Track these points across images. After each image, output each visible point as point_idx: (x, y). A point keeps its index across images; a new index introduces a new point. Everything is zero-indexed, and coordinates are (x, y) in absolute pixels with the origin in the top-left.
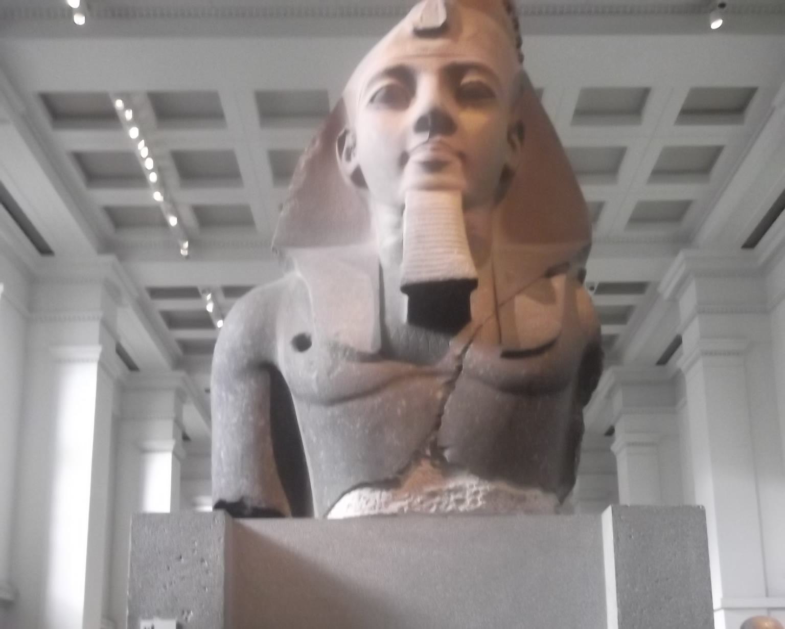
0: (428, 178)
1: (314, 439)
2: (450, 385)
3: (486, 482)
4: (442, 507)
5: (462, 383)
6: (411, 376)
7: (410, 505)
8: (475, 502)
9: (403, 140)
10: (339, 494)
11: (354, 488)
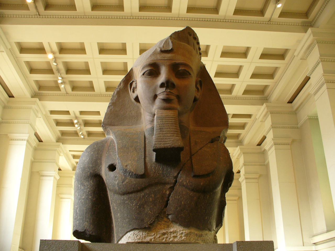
0: (165, 105)
1: (116, 208)
2: (172, 189)
3: (186, 229)
4: (167, 239)
5: (177, 187)
6: (156, 184)
8: (181, 237)
9: (155, 90)
11: (132, 230)
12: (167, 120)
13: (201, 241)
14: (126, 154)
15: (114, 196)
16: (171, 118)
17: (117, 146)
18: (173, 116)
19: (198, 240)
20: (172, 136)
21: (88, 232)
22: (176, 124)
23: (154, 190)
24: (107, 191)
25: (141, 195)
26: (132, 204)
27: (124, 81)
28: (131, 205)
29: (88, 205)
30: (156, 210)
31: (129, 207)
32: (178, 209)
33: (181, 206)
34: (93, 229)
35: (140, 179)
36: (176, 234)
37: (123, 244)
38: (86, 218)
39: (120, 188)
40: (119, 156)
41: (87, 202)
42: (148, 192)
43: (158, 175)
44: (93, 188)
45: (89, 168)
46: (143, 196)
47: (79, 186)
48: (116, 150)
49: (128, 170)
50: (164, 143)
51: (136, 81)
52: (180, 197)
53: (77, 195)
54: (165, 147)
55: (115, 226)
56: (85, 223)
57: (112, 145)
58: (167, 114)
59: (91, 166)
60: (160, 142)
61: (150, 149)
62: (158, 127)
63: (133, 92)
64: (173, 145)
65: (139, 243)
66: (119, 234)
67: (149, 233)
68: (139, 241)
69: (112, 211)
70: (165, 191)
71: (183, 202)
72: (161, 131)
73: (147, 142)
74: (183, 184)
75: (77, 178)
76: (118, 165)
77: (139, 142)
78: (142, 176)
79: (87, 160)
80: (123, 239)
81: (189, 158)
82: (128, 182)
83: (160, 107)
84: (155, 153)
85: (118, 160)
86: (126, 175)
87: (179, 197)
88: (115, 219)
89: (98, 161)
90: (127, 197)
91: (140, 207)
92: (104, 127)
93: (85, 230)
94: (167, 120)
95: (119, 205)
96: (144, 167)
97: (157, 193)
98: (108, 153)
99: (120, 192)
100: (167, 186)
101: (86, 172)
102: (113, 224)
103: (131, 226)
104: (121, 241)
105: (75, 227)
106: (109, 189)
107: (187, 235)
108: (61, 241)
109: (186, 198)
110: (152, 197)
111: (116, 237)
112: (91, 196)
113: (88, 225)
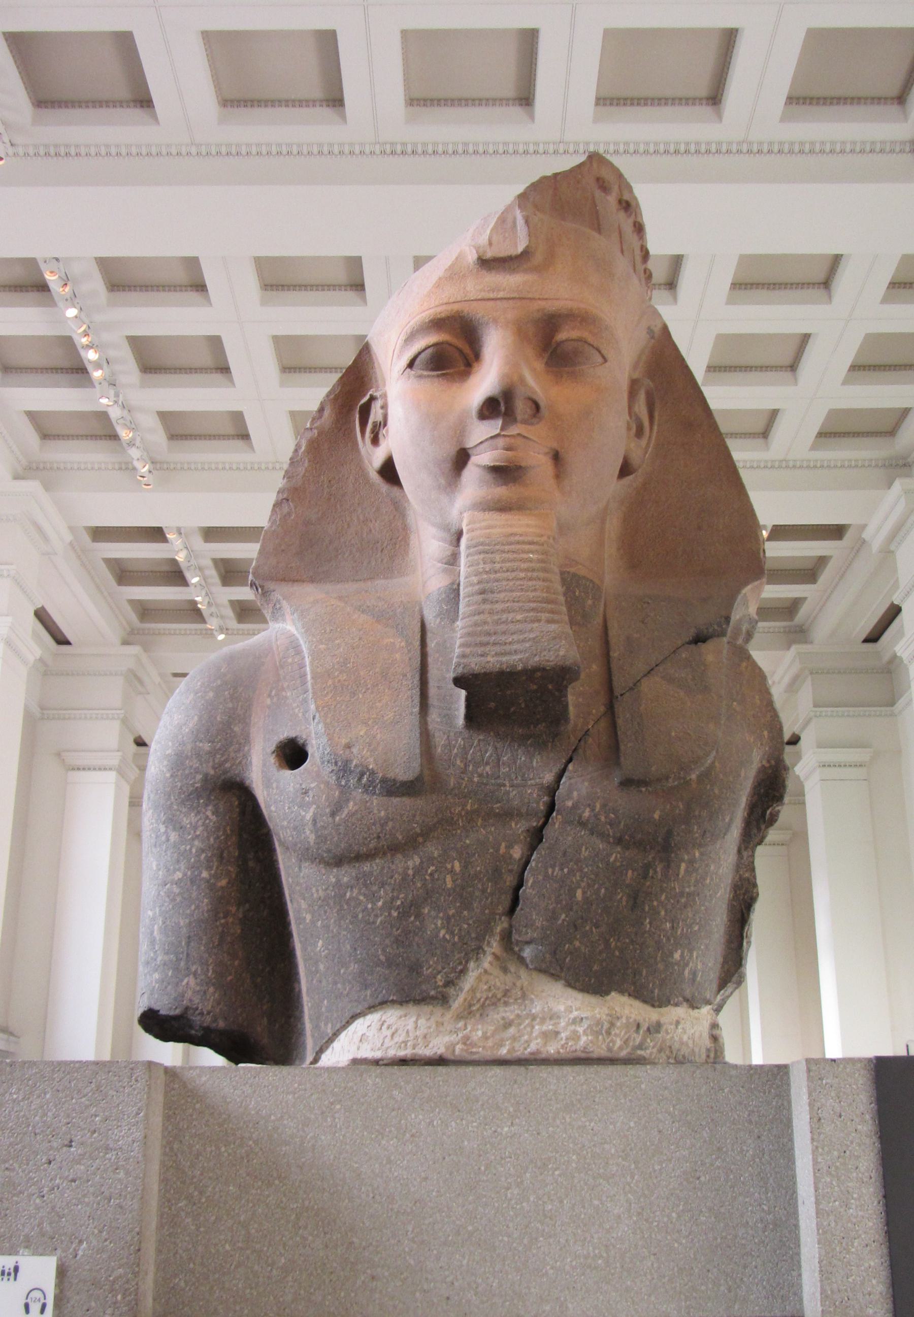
0: (501, 491)
1: (308, 917)
7: (466, 1040)
8: (575, 1037)
9: (461, 430)
10: (347, 1015)
11: (372, 1008)
12: (511, 556)
13: (655, 1050)
14: (348, 698)
15: (300, 867)
16: (527, 547)
17: (312, 663)
18: (536, 539)
19: (646, 1049)
20: (533, 621)
21: (199, 1018)
22: (545, 570)
23: (459, 846)
24: (274, 850)
25: (410, 863)
26: (374, 903)
27: (336, 399)
28: (370, 906)
29: (197, 907)
30: (469, 925)
31: (360, 916)
32: (560, 922)
33: (571, 909)
34: (219, 1004)
35: (404, 799)
36: (552, 1022)
37: (332, 1070)
38: (187, 962)
39: (321, 839)
40: (317, 708)
41: (194, 895)
42: (436, 854)
43: (476, 779)
44: (215, 839)
45: (198, 756)
46: (418, 870)
47: (163, 829)
48: (304, 683)
49: (354, 763)
50: (498, 649)
51: (385, 396)
52: (566, 870)
53: (155, 868)
54: (504, 667)
55: (308, 990)
56: (185, 981)
57: (290, 660)
58: (510, 530)
59: (207, 746)
60: (482, 649)
61: (442, 674)
62: (472, 585)
63: (375, 441)
64: (537, 659)
65: (403, 1062)
66: (323, 1025)
67: (440, 1020)
68: (402, 1053)
69: (294, 928)
70: (506, 847)
71: (579, 894)
72: (485, 601)
73: (431, 645)
74: (580, 817)
75: (152, 796)
76: (314, 742)
77: (398, 646)
78: (409, 788)
79: (191, 725)
80: (336, 1045)
81: (602, 709)
82: (351, 815)
83: (480, 503)
84: (463, 693)
85: (316, 721)
86: (346, 784)
87: (562, 870)
88: (305, 960)
89: (236, 729)
90: (354, 874)
91: (404, 914)
92: (260, 590)
93: (187, 1008)
94: (511, 556)
95: (320, 906)
96: (418, 751)
97: (474, 854)
98: (273, 693)
99: (325, 855)
100: (513, 825)
101: (187, 772)
102: (299, 983)
103: (369, 992)
104: (330, 1050)
105: (146, 996)
106: (279, 840)
107: (597, 1029)
108: (77, 1065)
109: (592, 876)
110: (452, 871)
111: (313, 1036)
112: (209, 868)
113: (198, 988)
